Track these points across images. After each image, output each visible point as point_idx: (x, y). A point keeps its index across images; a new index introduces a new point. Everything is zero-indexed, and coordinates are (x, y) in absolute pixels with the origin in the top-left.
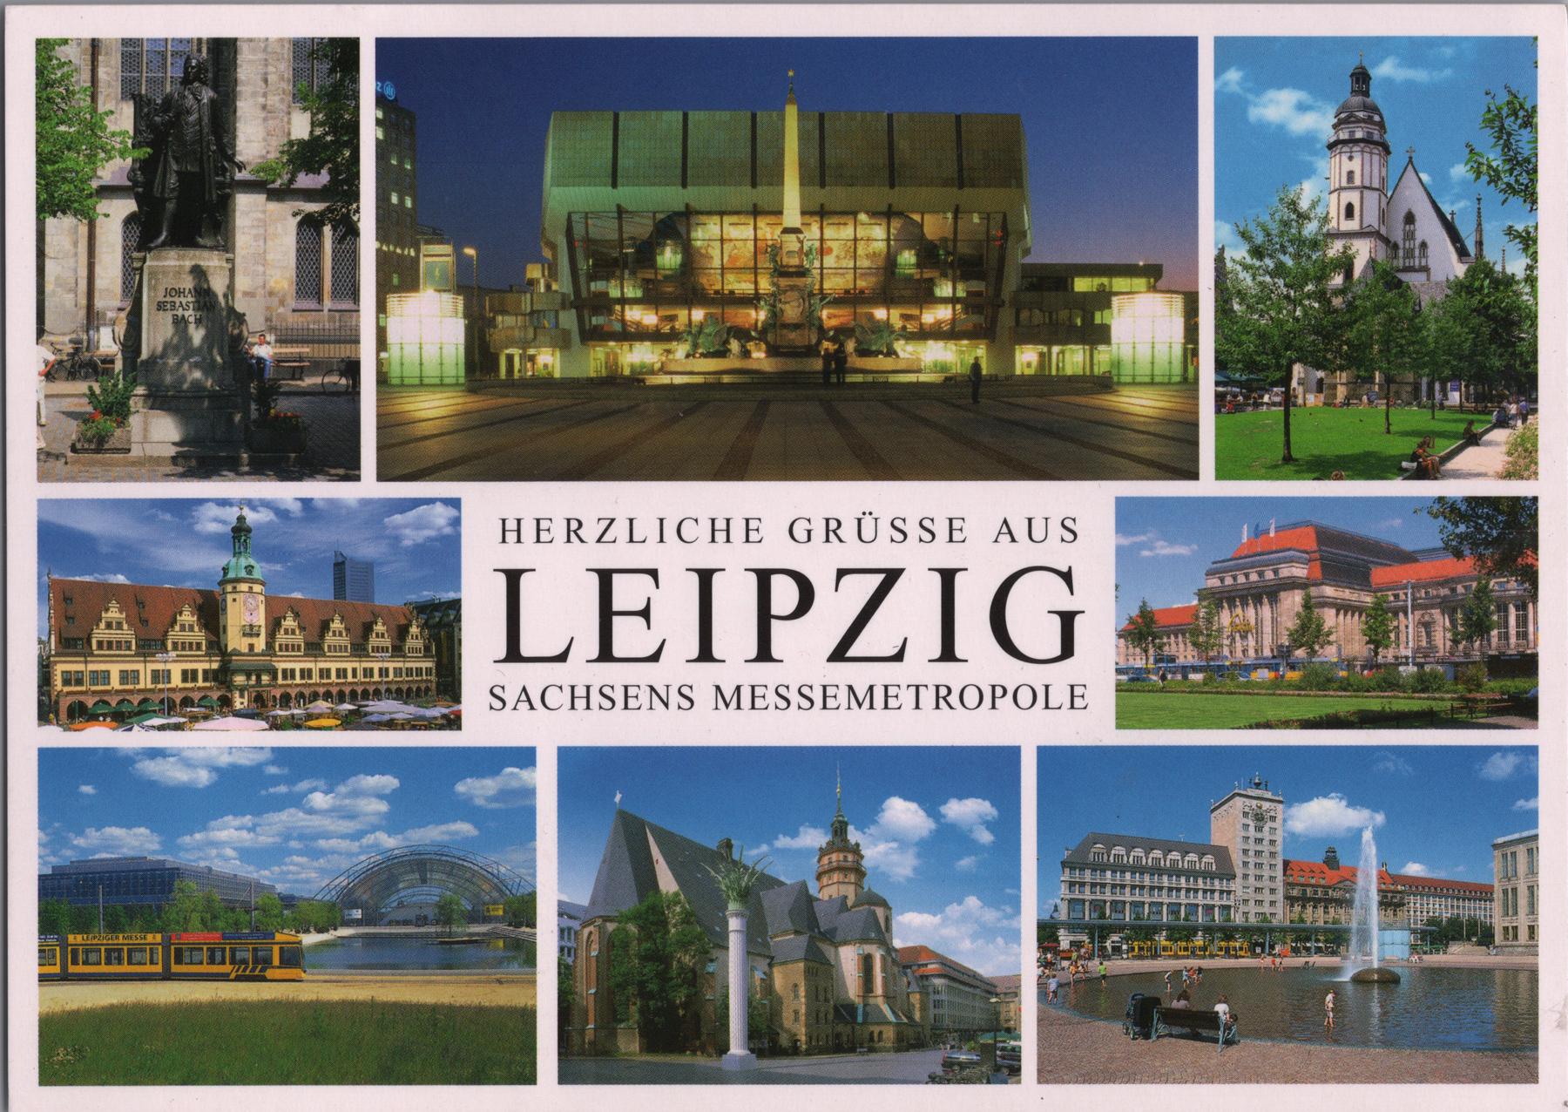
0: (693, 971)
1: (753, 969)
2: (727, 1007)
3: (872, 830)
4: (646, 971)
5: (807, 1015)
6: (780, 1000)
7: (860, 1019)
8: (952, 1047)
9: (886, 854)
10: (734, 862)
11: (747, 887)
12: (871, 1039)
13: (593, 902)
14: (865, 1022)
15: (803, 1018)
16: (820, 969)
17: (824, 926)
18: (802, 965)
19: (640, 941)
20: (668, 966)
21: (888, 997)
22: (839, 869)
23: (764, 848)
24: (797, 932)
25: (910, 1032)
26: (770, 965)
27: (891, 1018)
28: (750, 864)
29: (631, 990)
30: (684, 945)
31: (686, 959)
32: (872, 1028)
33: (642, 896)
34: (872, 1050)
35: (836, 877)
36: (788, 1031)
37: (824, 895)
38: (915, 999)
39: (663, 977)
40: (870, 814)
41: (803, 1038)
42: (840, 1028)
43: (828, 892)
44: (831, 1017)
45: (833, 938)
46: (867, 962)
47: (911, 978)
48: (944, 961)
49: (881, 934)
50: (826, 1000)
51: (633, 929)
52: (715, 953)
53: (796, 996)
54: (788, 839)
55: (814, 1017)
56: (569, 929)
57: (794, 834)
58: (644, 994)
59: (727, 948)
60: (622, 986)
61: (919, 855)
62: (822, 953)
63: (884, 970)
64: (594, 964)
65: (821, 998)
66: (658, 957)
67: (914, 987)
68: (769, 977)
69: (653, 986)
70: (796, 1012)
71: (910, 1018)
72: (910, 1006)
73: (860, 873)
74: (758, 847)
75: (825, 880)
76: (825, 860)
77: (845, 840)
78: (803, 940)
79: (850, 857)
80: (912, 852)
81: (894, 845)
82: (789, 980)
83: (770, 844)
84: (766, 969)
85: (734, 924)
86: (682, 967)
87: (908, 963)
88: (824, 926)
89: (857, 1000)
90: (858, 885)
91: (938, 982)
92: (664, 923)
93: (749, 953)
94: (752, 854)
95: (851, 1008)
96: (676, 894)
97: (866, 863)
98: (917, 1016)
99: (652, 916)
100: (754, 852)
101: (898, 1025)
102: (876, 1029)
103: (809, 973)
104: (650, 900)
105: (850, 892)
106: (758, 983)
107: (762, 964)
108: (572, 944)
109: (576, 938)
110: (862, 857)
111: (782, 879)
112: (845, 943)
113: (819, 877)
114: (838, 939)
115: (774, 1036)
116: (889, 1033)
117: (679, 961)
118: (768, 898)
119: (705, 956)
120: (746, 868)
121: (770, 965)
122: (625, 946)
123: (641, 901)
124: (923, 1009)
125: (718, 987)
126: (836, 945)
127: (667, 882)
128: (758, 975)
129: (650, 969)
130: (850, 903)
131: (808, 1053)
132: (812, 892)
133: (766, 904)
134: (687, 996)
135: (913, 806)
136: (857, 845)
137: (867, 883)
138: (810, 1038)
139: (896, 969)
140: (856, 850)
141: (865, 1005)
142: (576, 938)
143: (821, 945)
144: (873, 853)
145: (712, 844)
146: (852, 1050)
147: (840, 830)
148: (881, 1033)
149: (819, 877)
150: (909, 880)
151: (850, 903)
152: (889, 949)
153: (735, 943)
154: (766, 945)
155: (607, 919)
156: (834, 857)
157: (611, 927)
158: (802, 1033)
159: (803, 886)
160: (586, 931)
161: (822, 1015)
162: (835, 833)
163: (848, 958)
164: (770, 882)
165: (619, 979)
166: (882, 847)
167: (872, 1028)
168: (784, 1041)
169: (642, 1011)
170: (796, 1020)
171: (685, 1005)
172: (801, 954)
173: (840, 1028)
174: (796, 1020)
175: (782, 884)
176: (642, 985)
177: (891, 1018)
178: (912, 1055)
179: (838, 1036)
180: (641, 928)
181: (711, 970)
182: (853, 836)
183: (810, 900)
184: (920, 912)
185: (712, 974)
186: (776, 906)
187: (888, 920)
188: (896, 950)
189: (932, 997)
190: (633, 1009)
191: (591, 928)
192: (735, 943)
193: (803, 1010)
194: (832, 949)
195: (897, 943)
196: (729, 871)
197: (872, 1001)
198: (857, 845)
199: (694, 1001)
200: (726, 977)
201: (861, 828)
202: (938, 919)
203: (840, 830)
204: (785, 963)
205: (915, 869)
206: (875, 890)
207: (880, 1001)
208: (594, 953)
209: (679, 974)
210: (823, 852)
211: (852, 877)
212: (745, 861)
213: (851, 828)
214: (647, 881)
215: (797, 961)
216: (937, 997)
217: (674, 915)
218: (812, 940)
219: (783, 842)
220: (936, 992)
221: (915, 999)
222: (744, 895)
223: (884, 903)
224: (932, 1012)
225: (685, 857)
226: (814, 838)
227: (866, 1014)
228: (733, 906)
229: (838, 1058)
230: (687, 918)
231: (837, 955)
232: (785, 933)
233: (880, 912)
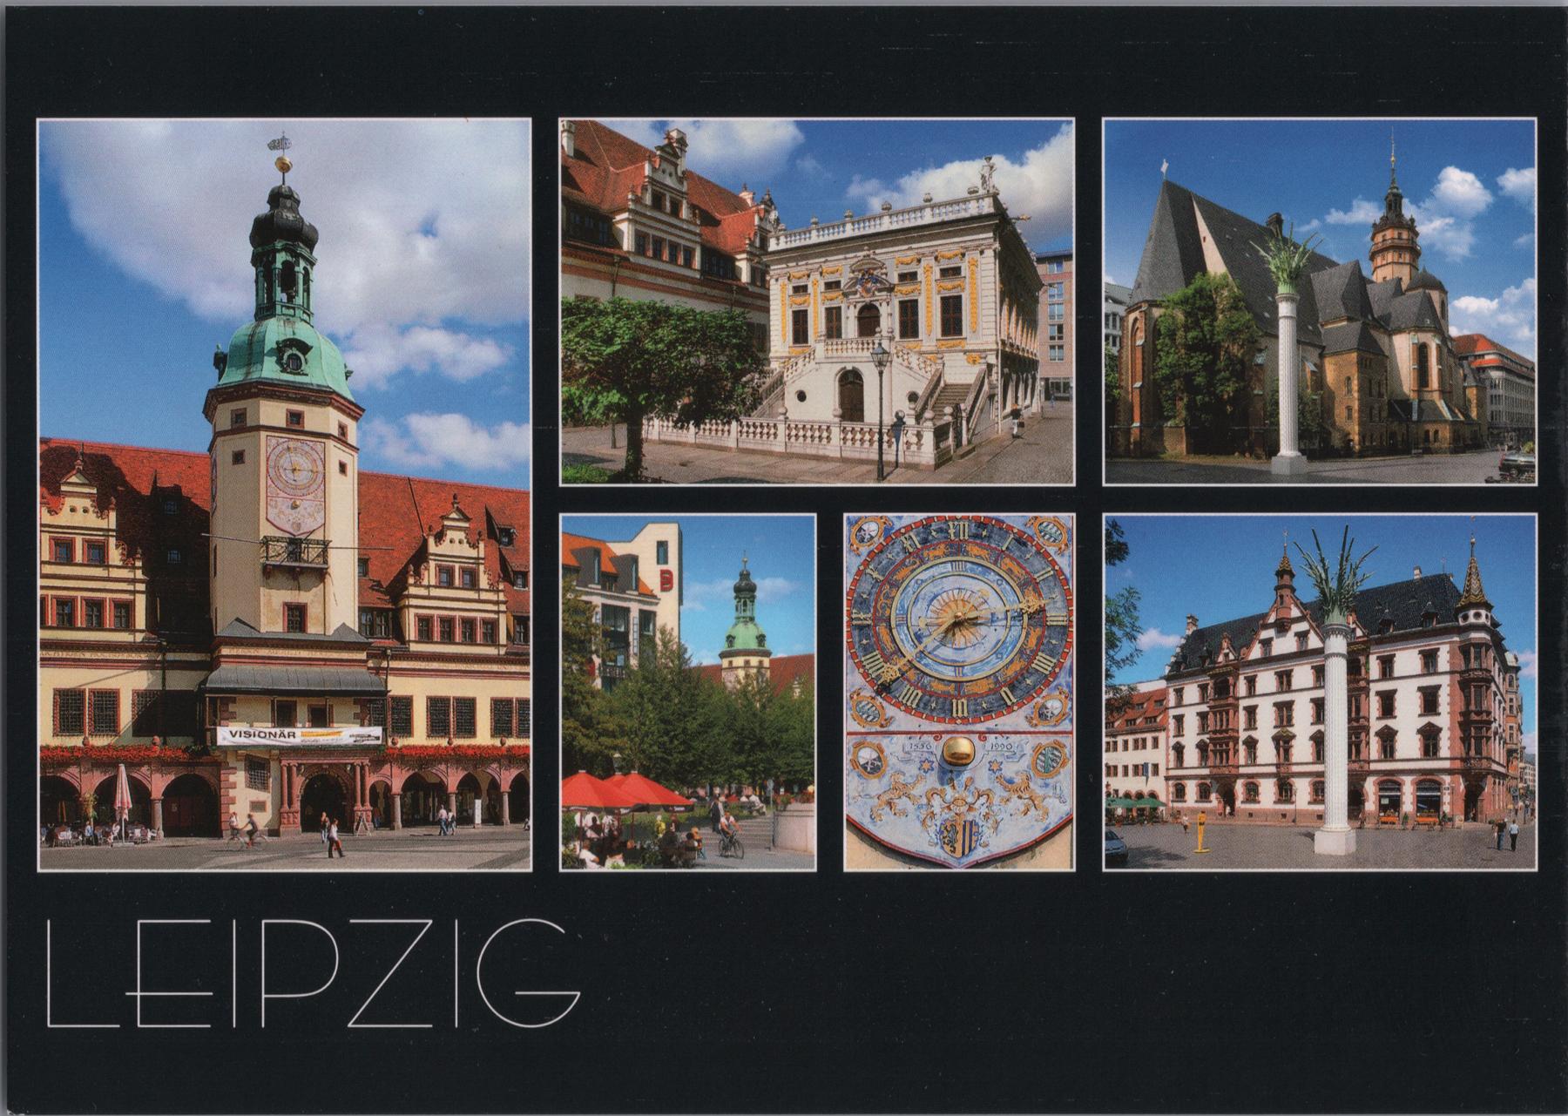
0: (1242, 362)
1: (1304, 360)
2: (1277, 403)
3: (1428, 204)
4: (1193, 362)
5: (1360, 411)
7: (1415, 417)
9: (1443, 231)
10: (1285, 241)
11: (1298, 266)
13: (1139, 286)
14: (1419, 421)
15: (1356, 415)
16: (1374, 361)
17: (1377, 312)
18: (1354, 355)
20: (1216, 357)
21: (1445, 392)
23: (1315, 223)
24: (1350, 319)
26: (1322, 356)
27: (1448, 416)
28: (1300, 241)
29: (1177, 383)
31: (1235, 349)
33: (1188, 281)
34: (1428, 451)
35: (1390, 257)
37: (1377, 277)
38: (1472, 393)
39: (1210, 368)
40: (1426, 185)
41: (1356, 438)
42: (1395, 426)
43: (1384, 272)
44: (1384, 414)
45: (1388, 326)
46: (1422, 350)
47: (1467, 371)
48: (1502, 353)
49: (1434, 319)
50: (1380, 395)
51: (1180, 317)
52: (1264, 342)
54: (1341, 214)
56: (1115, 315)
57: (1347, 208)
58: (1190, 388)
59: (1277, 337)
60: (1168, 379)
61: (1475, 233)
63: (1440, 361)
64: (1139, 355)
65: (1374, 392)
67: (1471, 381)
68: (1320, 368)
70: (1349, 409)
71: (1467, 416)
72: (1467, 401)
73: (1415, 252)
74: (1309, 223)
75: (1379, 261)
76: (1379, 238)
77: (1400, 215)
78: (1357, 326)
79: (1405, 235)
80: (1468, 227)
81: (1450, 221)
82: (1340, 371)
83: (1322, 220)
84: (1317, 361)
85: (1285, 309)
86: (1231, 359)
87: (1460, 352)
88: (1377, 312)
89: (1412, 396)
90: (1413, 266)
91: (1495, 374)
92: (1211, 310)
93: (1299, 342)
94: (1302, 230)
95: (1405, 404)
96: (1224, 277)
97: (1420, 241)
98: (1474, 414)
99: (1201, 305)
100: (1305, 228)
101: (1453, 423)
102: (1431, 428)
103: (1363, 365)
105: (1404, 273)
107: (1314, 354)
108: (1117, 332)
109: (1122, 327)
110: (1417, 234)
111: (1334, 258)
112: (1399, 331)
113: (1372, 257)
114: (1392, 326)
115: (1325, 435)
116: (1446, 433)
119: (1253, 346)
120: (1296, 247)
121: (1322, 356)
122: (1172, 335)
123: (1188, 284)
126: (1390, 334)
127: (1215, 263)
128: (1310, 367)
129: (1197, 360)
130: (1404, 287)
131: (1362, 455)
132: (1365, 273)
133: (1317, 286)
134: (1235, 392)
135: (1470, 177)
136: (1412, 220)
137: (1421, 263)
139: (1451, 360)
140: (1411, 227)
141: (1420, 401)
142: (1122, 327)
143: (1374, 333)
144: (1429, 229)
145: (1261, 218)
146: (1406, 451)
147: (1394, 203)
148: (1436, 432)
150: (1466, 260)
151: (1404, 287)
152: (1445, 338)
153: (1285, 330)
155: (1153, 304)
156: (1389, 234)
157: (1157, 312)
158: (1354, 430)
160: (1132, 317)
161: (1375, 412)
162: (1389, 207)
163: (1403, 347)
164: (1319, 262)
165: (1166, 371)
166: (1438, 223)
168: (1336, 441)
169: (1188, 408)
170: (1350, 417)
171: (1232, 401)
172: (1354, 342)
175: (1333, 264)
176: (1188, 378)
177: (1448, 416)
178: (1466, 458)
179: (1393, 435)
180: (1187, 314)
181: (1259, 360)
182: (1408, 210)
184: (1477, 296)
186: (1329, 285)
187: (1443, 305)
188: (1451, 339)
189: (1490, 392)
190: (1180, 405)
191: (1136, 314)
192: (1285, 331)
193: (1356, 406)
194: (1386, 339)
195: (1454, 332)
196: (1279, 250)
197: (1427, 396)
198: (1412, 220)
199: (1242, 397)
201: (1416, 201)
202: (1494, 304)
203: (1394, 203)
205: (1473, 249)
206: (1430, 271)
207: (1436, 396)
208: (1139, 342)
209: (1227, 366)
210: (1378, 228)
211: (1407, 257)
212: (1295, 239)
213: (1405, 201)
214: (1193, 261)
215: (1350, 351)
216: (1494, 392)
217: (1223, 299)
219: (1335, 217)
220: (1494, 386)
221: (1472, 393)
222: (1296, 277)
223: (1439, 287)
224: (1490, 408)
225: (1240, 238)
226: (1368, 212)
228: (1283, 289)
229: (1390, 460)
231: (1391, 345)
233: (1435, 296)
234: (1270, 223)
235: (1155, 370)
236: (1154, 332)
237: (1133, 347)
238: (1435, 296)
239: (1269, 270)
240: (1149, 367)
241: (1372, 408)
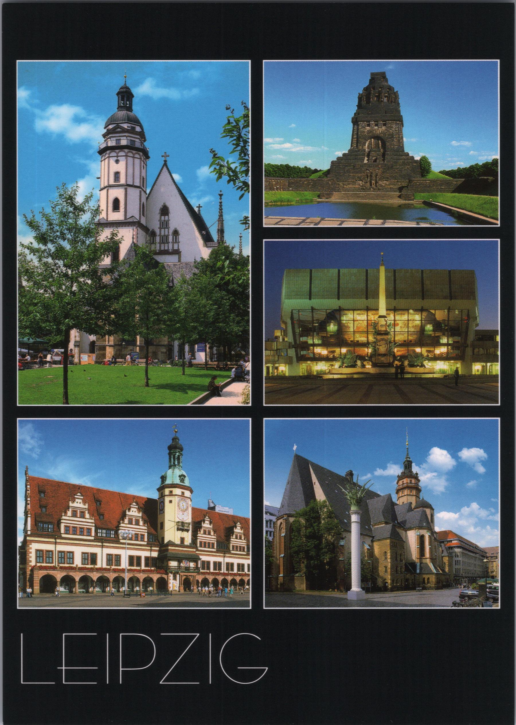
2: (350, 564)
3: (424, 466)
4: (309, 544)
5: (391, 568)
6: (377, 560)
7: (418, 571)
8: (465, 587)
9: (431, 479)
12: (424, 582)
13: (282, 506)
14: (420, 574)
15: (389, 570)
16: (398, 544)
17: (400, 520)
18: (388, 541)
19: (306, 528)
20: (321, 542)
22: (408, 487)
24: (386, 523)
25: (443, 578)
26: (372, 541)
29: (301, 555)
30: (329, 530)
32: (424, 576)
33: (307, 503)
34: (424, 588)
35: (406, 492)
36: (382, 578)
37: (400, 502)
39: (318, 547)
41: (389, 581)
42: (408, 576)
43: (402, 500)
44: (403, 570)
45: (404, 526)
46: (421, 538)
50: (401, 560)
51: (303, 521)
52: (344, 534)
53: (386, 558)
55: (395, 569)
56: (271, 521)
58: (309, 558)
59: (350, 532)
60: (297, 553)
62: (398, 533)
63: (430, 544)
65: (398, 559)
66: (315, 536)
68: (372, 547)
69: (313, 553)
70: (386, 567)
71: (443, 571)
73: (418, 490)
75: (400, 494)
77: (411, 471)
78: (389, 527)
79: (413, 481)
82: (381, 549)
85: (354, 518)
86: (328, 543)
88: (400, 520)
89: (417, 561)
90: (417, 496)
92: (318, 518)
93: (361, 534)
95: (413, 565)
96: (325, 502)
97: (420, 484)
102: (426, 577)
104: (312, 505)
105: (413, 500)
106: (366, 551)
107: (368, 540)
110: (419, 481)
111: (379, 493)
112: (410, 529)
114: (408, 525)
115: (374, 580)
116: (433, 579)
117: (326, 539)
118: (372, 504)
119: (339, 536)
121: (372, 541)
122: (299, 531)
124: (450, 565)
125: (346, 554)
126: (406, 530)
127: (320, 495)
128: (367, 547)
129: (311, 543)
130: (413, 506)
131: (392, 590)
132: (394, 500)
134: (330, 559)
136: (417, 474)
137: (421, 495)
138: (393, 581)
140: (416, 477)
141: (421, 563)
143: (398, 530)
146: (414, 589)
147: (408, 465)
148: (428, 579)
149: (397, 492)
151: (413, 506)
152: (433, 532)
153: (355, 529)
154: (370, 530)
155: (290, 515)
156: (405, 480)
157: (291, 520)
159: (389, 497)
161: (399, 569)
162: (406, 467)
163: (412, 537)
164: (372, 495)
165: (296, 549)
166: (429, 475)
167: (424, 576)
168: (380, 583)
169: (307, 567)
170: (386, 571)
171: (328, 563)
172: (388, 534)
173: (408, 576)
174: (386, 571)
175: (378, 496)
176: (307, 552)
179: (407, 580)
180: (307, 520)
182: (415, 469)
183: (393, 504)
185: (342, 546)
186: (376, 507)
187: (432, 516)
190: (303, 565)
191: (281, 520)
192: (355, 529)
193: (389, 566)
197: (424, 561)
198: (417, 474)
199: (333, 562)
200: (349, 548)
201: (419, 465)
203: (408, 465)
204: (379, 540)
206: (425, 499)
207: (428, 561)
210: (400, 478)
211: (414, 492)
213: (413, 464)
214: (309, 494)
215: (387, 539)
217: (324, 513)
218: (394, 526)
222: (359, 502)
223: (430, 506)
226: (395, 470)
227: (421, 569)
228: (353, 508)
230: (330, 515)
231: (406, 536)
232: (380, 523)
233: (428, 511)
234: (347, 475)
235: (290, 548)
236: (290, 529)
237: (280, 536)
238: (428, 511)
239: (346, 499)
240: (287, 548)
241: (397, 567)
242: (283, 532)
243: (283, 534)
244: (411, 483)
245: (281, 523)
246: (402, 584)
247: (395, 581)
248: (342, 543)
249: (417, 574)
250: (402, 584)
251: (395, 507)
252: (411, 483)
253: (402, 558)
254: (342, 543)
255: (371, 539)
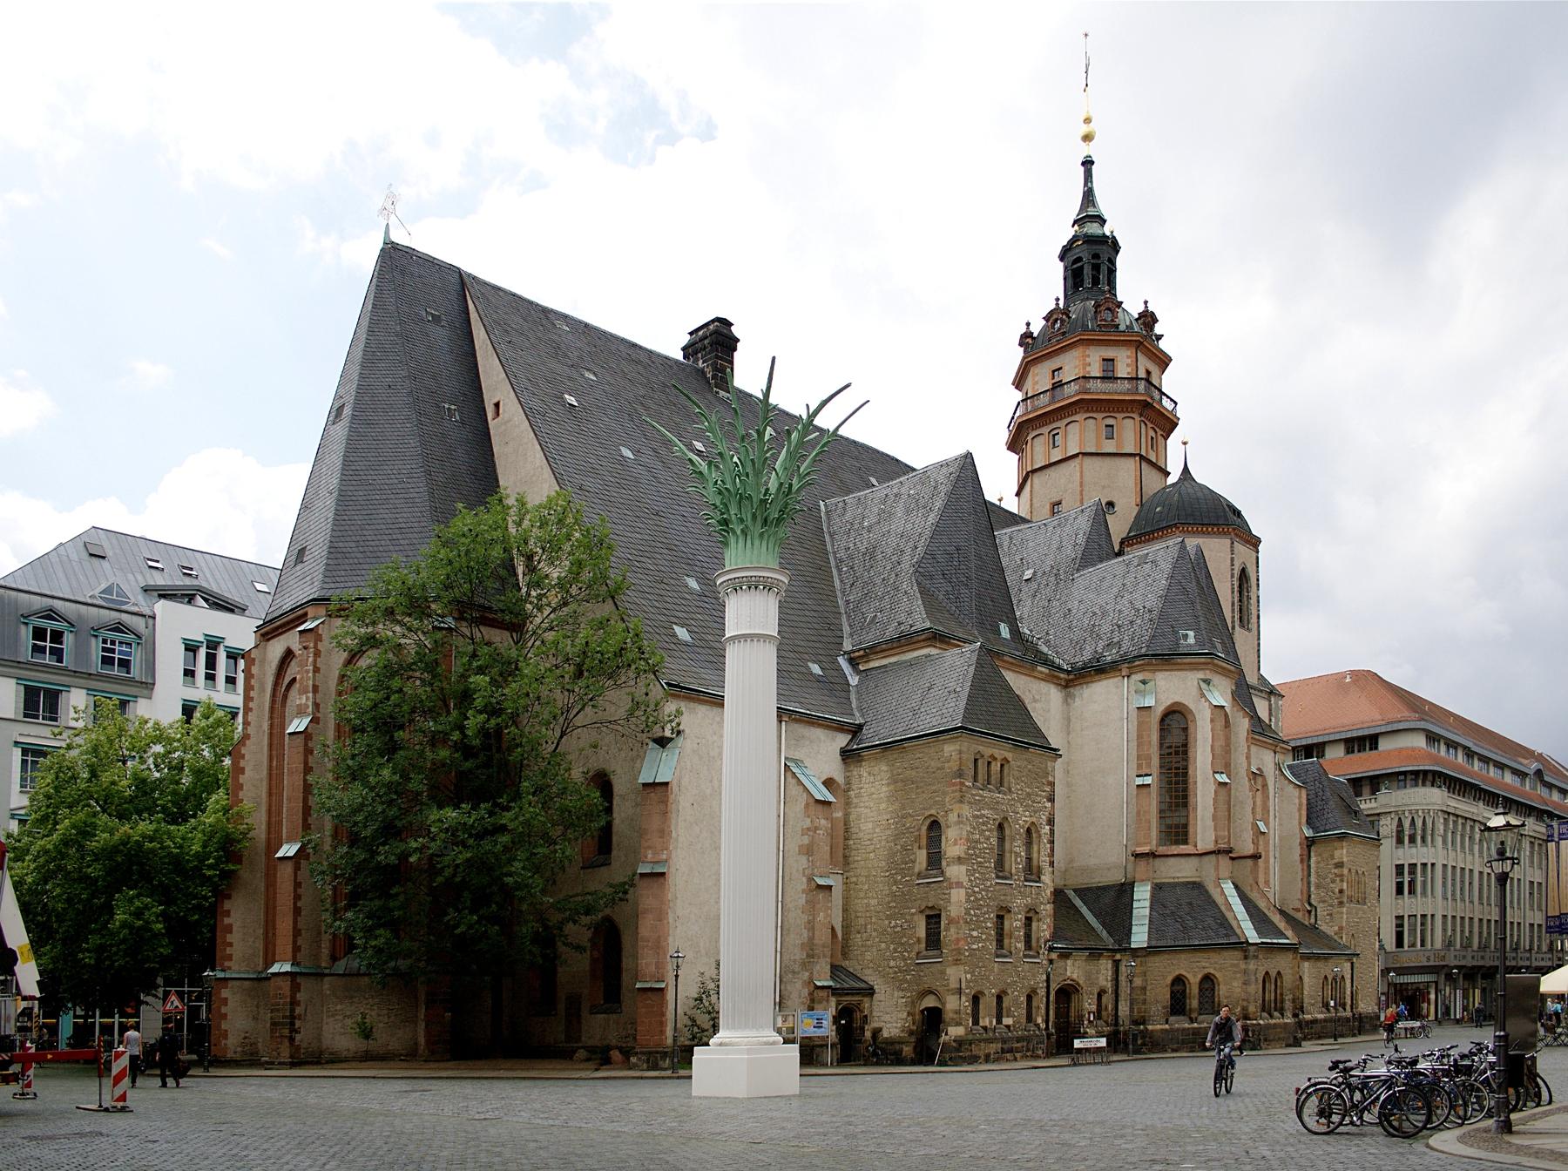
35: (1078, 434)
44: (1043, 929)
50: (1032, 872)
65: (1015, 864)
75: (1040, 451)
76: (1041, 379)
110: (1163, 361)
151: (1119, 526)
159: (966, 468)
161: (1015, 923)
162: (1074, 279)
173: (1074, 970)
179: (1067, 993)
194: (1054, 694)
206: (1199, 476)
211: (1129, 433)
218: (990, 657)
242: (301, 712)
243: (298, 725)
244: (1109, 377)
245: (289, 654)
246: (1029, 1018)
247: (988, 1003)
248: (660, 766)
249: (1135, 952)
250: (1029, 1018)
251: (1003, 534)
252: (1109, 377)
253: (1041, 856)
254: (660, 766)
255: (842, 740)
